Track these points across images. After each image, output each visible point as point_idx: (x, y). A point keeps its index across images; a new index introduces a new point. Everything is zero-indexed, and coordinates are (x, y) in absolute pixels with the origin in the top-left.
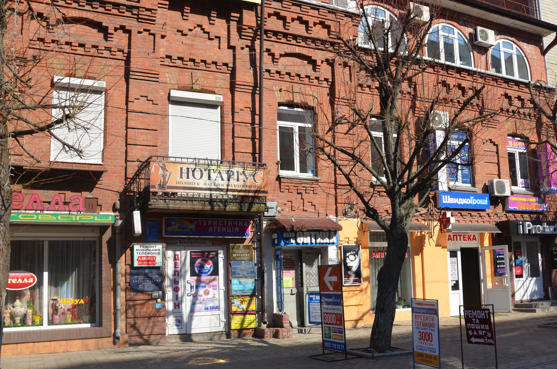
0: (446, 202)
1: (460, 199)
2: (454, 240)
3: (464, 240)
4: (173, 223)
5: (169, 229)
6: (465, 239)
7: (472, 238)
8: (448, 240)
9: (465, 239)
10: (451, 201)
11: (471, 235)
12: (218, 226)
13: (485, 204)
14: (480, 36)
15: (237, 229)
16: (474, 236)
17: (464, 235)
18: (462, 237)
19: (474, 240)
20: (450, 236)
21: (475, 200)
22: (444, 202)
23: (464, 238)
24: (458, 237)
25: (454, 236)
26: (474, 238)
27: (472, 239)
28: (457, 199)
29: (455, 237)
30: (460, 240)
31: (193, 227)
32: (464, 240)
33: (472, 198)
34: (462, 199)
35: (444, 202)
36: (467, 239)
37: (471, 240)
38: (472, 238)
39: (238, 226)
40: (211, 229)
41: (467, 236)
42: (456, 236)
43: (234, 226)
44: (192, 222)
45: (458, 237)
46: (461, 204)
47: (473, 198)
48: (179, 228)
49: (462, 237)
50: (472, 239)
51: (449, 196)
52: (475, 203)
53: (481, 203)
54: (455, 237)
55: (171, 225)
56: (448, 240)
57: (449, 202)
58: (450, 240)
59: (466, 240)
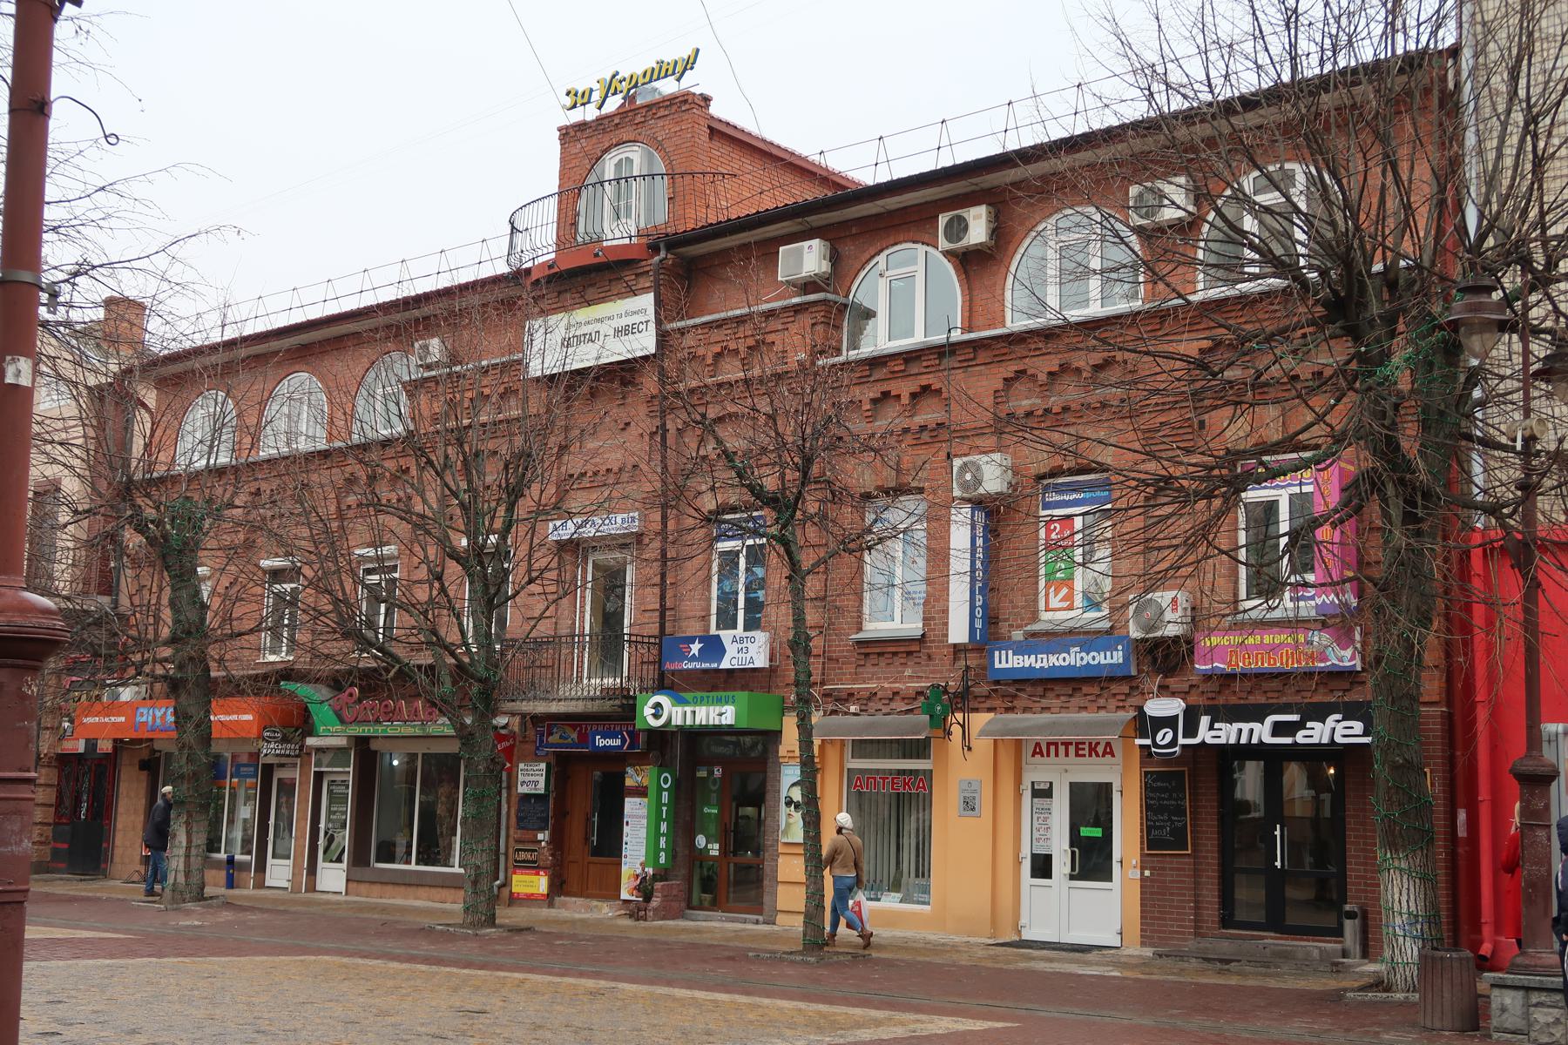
0: (1004, 665)
2: (1048, 755)
3: (1077, 755)
5: (550, 739)
7: (1100, 749)
10: (1016, 661)
11: (1098, 743)
13: (1114, 661)
16: (1108, 744)
17: (1077, 744)
18: (1072, 749)
20: (1038, 744)
21: (1083, 654)
22: (997, 665)
23: (1077, 749)
24: (1062, 749)
25: (1049, 744)
26: (1109, 750)
29: (1052, 748)
30: (1067, 755)
31: (574, 736)
32: (1077, 755)
33: (1073, 650)
34: (1045, 656)
35: (997, 665)
37: (1097, 755)
38: (1100, 749)
41: (1087, 747)
42: (1056, 744)
44: (574, 727)
45: (1062, 749)
47: (1077, 649)
48: (561, 737)
49: (1072, 749)
51: (1010, 652)
52: (1085, 662)
53: (1103, 662)
54: (1052, 748)
57: (1009, 665)
58: (1038, 756)
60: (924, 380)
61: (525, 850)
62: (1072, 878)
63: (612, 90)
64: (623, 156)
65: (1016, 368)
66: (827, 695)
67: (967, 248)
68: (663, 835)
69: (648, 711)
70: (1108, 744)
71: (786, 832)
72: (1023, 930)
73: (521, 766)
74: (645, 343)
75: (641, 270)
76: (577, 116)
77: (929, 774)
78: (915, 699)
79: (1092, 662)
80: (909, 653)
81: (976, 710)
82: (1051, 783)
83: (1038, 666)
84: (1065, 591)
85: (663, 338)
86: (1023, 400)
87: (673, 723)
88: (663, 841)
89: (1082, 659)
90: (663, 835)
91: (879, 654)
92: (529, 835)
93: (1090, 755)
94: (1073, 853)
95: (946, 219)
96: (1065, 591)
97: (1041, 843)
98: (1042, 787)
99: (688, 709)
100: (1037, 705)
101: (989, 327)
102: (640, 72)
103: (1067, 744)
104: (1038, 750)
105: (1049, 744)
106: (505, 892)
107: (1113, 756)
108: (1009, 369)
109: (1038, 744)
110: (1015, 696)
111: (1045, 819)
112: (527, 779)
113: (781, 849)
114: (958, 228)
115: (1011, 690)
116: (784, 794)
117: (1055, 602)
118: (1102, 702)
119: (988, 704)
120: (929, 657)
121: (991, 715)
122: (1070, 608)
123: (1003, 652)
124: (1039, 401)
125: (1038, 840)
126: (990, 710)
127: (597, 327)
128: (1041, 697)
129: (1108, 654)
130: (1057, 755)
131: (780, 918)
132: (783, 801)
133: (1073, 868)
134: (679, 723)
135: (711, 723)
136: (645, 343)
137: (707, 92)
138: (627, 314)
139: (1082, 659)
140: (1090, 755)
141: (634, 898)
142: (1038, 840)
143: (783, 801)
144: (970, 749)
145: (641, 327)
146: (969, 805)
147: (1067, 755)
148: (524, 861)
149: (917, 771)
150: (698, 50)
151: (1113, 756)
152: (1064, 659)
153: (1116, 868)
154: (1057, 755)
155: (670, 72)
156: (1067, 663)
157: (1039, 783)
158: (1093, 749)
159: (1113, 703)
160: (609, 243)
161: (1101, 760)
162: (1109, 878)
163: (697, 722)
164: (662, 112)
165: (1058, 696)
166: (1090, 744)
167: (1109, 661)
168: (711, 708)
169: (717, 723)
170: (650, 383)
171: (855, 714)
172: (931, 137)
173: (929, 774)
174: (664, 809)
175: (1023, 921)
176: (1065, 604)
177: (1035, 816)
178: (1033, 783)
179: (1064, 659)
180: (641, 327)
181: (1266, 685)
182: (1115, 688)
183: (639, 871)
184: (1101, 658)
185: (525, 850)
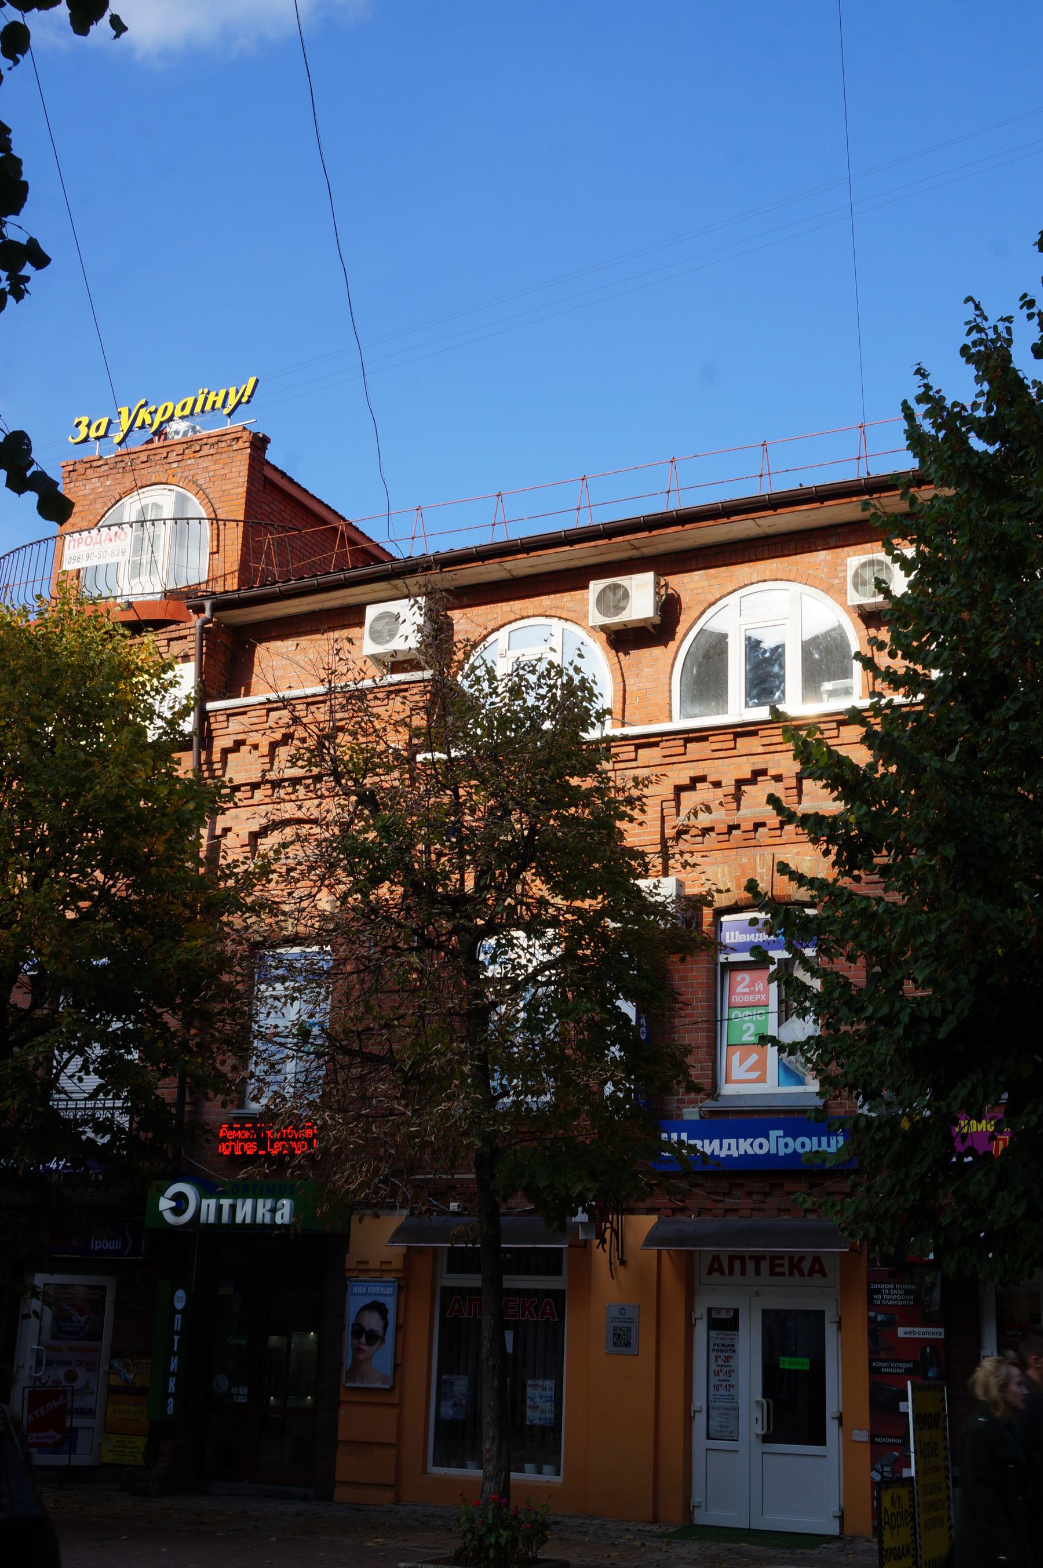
1: (726, 1142)
2: (731, 1273)
3: (772, 1273)
6: (777, 1270)
7: (806, 1266)
8: (709, 1273)
9: (777, 1270)
11: (802, 1258)
17: (774, 1258)
18: (765, 1265)
19: (817, 1276)
20: (716, 1258)
21: (789, 1140)
24: (750, 1265)
26: (818, 1267)
27: (806, 1272)
28: (716, 1142)
29: (737, 1264)
30: (758, 1273)
32: (772, 1273)
33: (773, 1134)
34: (733, 1142)
36: (786, 1269)
37: (802, 1274)
38: (806, 1266)
41: (786, 1262)
42: (742, 1258)
45: (750, 1265)
46: (729, 1157)
47: (781, 1133)
49: (765, 1265)
50: (806, 1272)
52: (789, 1151)
54: (737, 1264)
56: (709, 1273)
58: (716, 1275)
59: (782, 1274)
62: (766, 1439)
63: (138, 423)
65: (693, 774)
67: (625, 624)
68: (173, 1374)
69: (165, 1204)
70: (817, 1259)
71: (352, 1374)
72: (697, 1512)
77: (558, 1297)
79: (800, 1150)
81: (633, 1211)
82: (736, 1311)
83: (723, 1154)
84: (754, 1058)
87: (203, 1218)
88: (172, 1382)
89: (786, 1145)
90: (173, 1374)
93: (791, 1274)
95: (601, 587)
96: (754, 1058)
97: (722, 1391)
98: (723, 1315)
99: (226, 1203)
100: (719, 1205)
101: (642, 722)
103: (758, 1259)
104: (716, 1266)
105: (732, 1259)
107: (824, 1275)
109: (716, 1258)
111: (727, 1359)
113: (343, 1396)
114: (618, 598)
116: (350, 1318)
117: (738, 1071)
119: (648, 1203)
121: (653, 1219)
122: (762, 1079)
125: (717, 1387)
126: (649, 1211)
128: (725, 1195)
129: (824, 1139)
130: (743, 1273)
131: (340, 1493)
132: (349, 1329)
134: (212, 1219)
135: (259, 1220)
137: (263, 430)
139: (786, 1145)
140: (791, 1274)
142: (717, 1387)
143: (349, 1329)
144: (623, 1262)
146: (622, 1338)
147: (758, 1273)
151: (824, 1275)
152: (761, 1146)
153: (832, 1428)
154: (743, 1273)
155: (218, 405)
156: (763, 1151)
157: (719, 1310)
158: (795, 1265)
162: (820, 1439)
163: (239, 1219)
165: (749, 1194)
166: (791, 1258)
168: (260, 1202)
169: (268, 1220)
171: (454, 1214)
174: (176, 1338)
175: (697, 1498)
176: (754, 1075)
177: (713, 1355)
178: (710, 1310)
179: (761, 1146)
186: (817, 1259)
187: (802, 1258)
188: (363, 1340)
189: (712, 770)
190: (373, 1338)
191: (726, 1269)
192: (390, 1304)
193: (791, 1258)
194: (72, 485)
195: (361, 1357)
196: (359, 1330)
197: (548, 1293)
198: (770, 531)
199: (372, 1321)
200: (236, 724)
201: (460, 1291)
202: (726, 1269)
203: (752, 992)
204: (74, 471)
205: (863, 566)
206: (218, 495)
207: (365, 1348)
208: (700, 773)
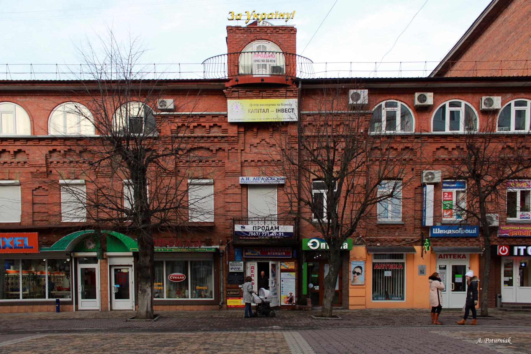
0: (436, 233)
2: (444, 258)
3: (454, 258)
4: (249, 250)
5: (247, 254)
7: (461, 256)
11: (461, 255)
12: (273, 251)
14: (485, 104)
15: (284, 253)
18: (452, 256)
19: (464, 258)
20: (441, 255)
24: (449, 256)
25: (444, 255)
26: (464, 256)
29: (446, 256)
30: (450, 258)
32: (454, 258)
34: (450, 231)
35: (434, 233)
36: (457, 257)
37: (460, 258)
38: (461, 256)
39: (284, 251)
40: (269, 254)
41: (457, 256)
42: (447, 255)
43: (282, 252)
45: (449, 256)
49: (452, 256)
51: (439, 229)
54: (446, 256)
55: (247, 252)
57: (438, 233)
58: (441, 258)
60: (406, 145)
61: (233, 291)
62: (452, 291)
64: (261, 44)
66: (367, 240)
70: (464, 255)
73: (230, 263)
74: (294, 117)
75: (289, 89)
76: (234, 24)
78: (401, 242)
80: (398, 228)
82: (446, 266)
83: (448, 233)
85: (300, 115)
86: (443, 155)
91: (386, 228)
92: (234, 286)
94: (453, 284)
95: (419, 95)
98: (443, 267)
102: (268, 13)
103: (450, 255)
104: (440, 257)
105: (444, 255)
106: (225, 306)
107: (465, 258)
108: (439, 145)
109: (441, 255)
110: (437, 241)
111: (443, 275)
112: (234, 267)
113: (350, 286)
115: (436, 239)
118: (466, 243)
120: (406, 230)
123: (436, 229)
124: (447, 156)
127: (267, 107)
130: (447, 258)
133: (453, 289)
136: (294, 117)
138: (282, 105)
141: (287, 304)
143: (352, 272)
145: (290, 110)
147: (450, 258)
148: (233, 295)
149: (398, 263)
150: (294, 12)
157: (441, 266)
158: (459, 256)
159: (469, 244)
160: (256, 76)
161: (461, 259)
164: (281, 32)
165: (452, 242)
166: (458, 255)
167: (471, 232)
170: (294, 131)
172: (397, 67)
173: (403, 264)
180: (290, 110)
181: (517, 240)
182: (471, 240)
183: (289, 295)
184: (468, 231)
185: (233, 291)
186: (464, 255)
187: (461, 255)
188: (356, 274)
189: (446, 145)
190: (358, 274)
191: (443, 257)
192: (363, 267)
193: (458, 255)
194: (231, 34)
195: (355, 278)
196: (354, 273)
197: (401, 263)
198: (462, 86)
199: (358, 270)
200: (308, 118)
201: (378, 263)
202: (443, 257)
203: (448, 197)
204: (231, 29)
205: (487, 99)
206: (286, 47)
207: (357, 276)
208: (443, 146)
